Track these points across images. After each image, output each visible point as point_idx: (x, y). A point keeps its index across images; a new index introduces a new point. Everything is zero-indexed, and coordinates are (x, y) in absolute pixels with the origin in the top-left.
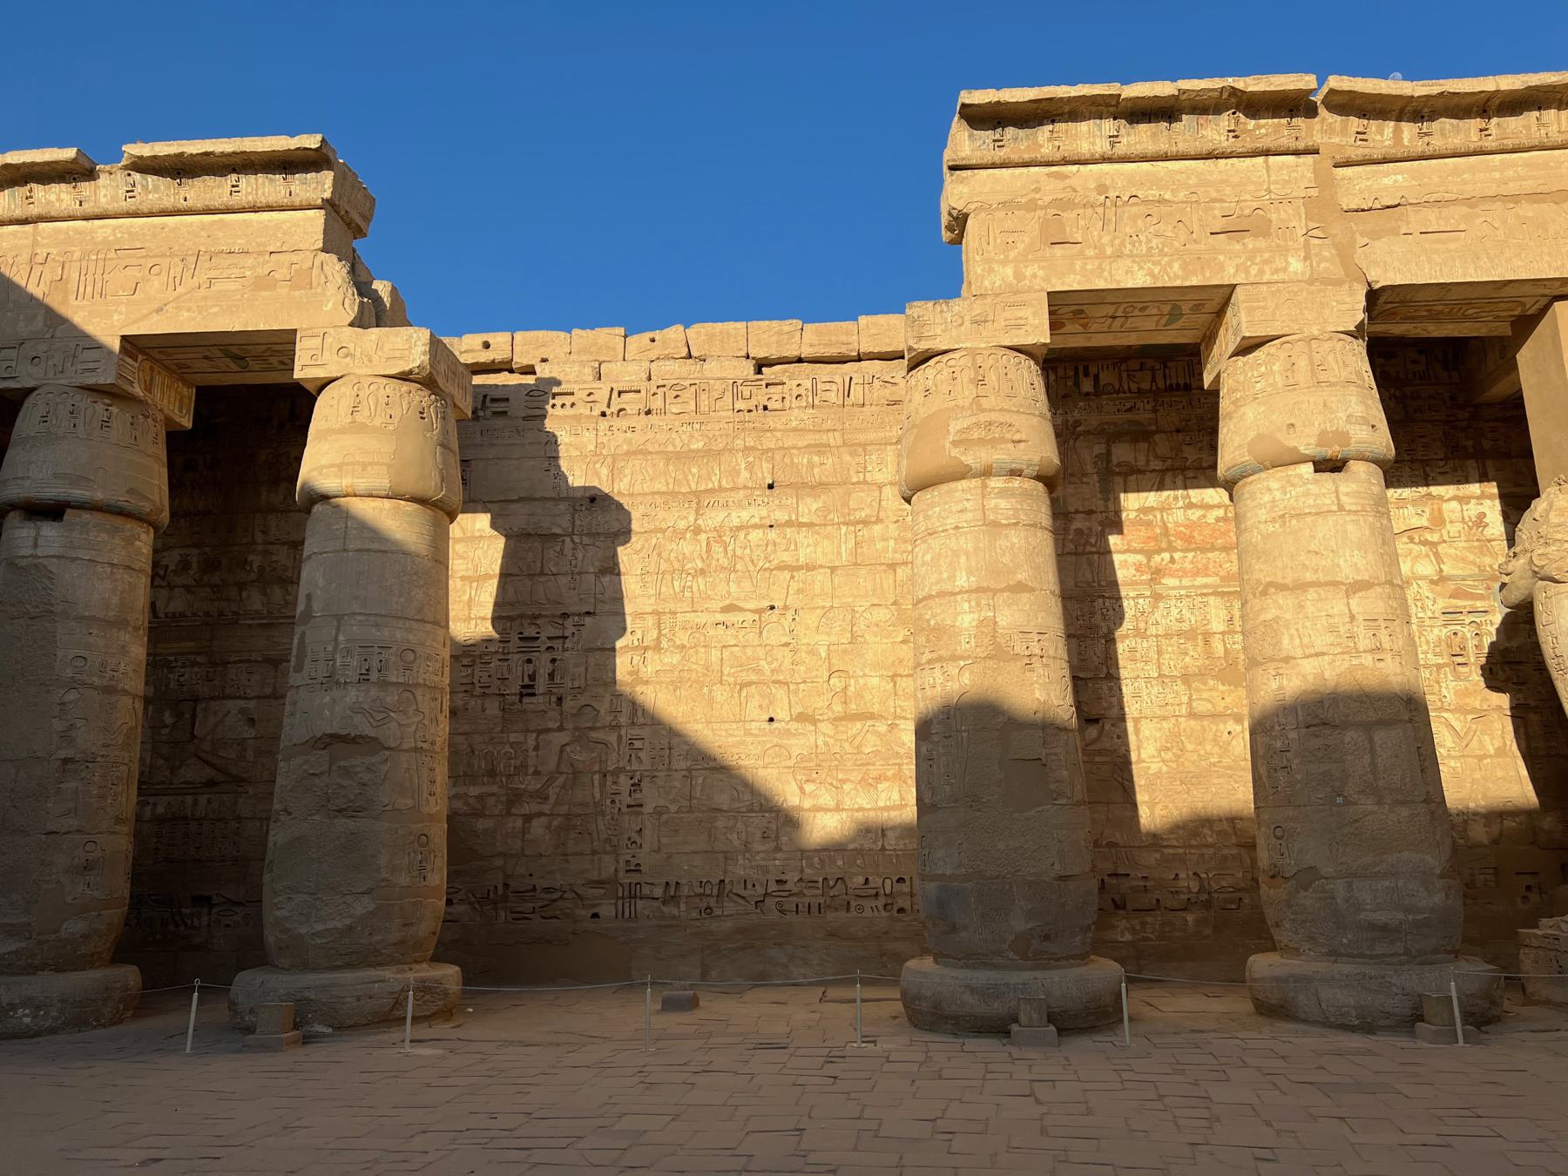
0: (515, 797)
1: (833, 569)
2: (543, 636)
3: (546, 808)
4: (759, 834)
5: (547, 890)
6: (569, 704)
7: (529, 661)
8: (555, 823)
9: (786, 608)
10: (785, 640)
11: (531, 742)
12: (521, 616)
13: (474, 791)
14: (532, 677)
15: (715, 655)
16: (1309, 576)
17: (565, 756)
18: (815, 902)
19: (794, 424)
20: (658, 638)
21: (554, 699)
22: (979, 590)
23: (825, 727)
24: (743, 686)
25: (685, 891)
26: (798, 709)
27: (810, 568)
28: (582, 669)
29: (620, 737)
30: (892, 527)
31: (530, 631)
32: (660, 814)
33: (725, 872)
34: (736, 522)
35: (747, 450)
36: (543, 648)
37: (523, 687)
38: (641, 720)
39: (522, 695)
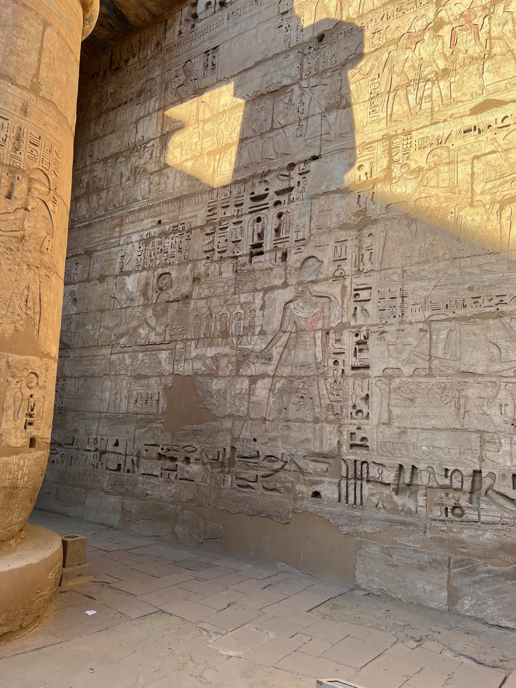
0: (243, 358)
2: (271, 193)
3: (270, 369)
5: (270, 458)
6: (293, 259)
7: (259, 220)
8: (278, 385)
11: (258, 302)
12: (253, 177)
13: (211, 352)
14: (260, 236)
15: (463, 170)
17: (288, 311)
20: (389, 169)
21: (279, 255)
25: (423, 479)
28: (307, 218)
29: (344, 287)
31: (260, 190)
32: (391, 378)
33: (482, 460)
36: (271, 205)
37: (254, 246)
38: (368, 266)
39: (252, 255)
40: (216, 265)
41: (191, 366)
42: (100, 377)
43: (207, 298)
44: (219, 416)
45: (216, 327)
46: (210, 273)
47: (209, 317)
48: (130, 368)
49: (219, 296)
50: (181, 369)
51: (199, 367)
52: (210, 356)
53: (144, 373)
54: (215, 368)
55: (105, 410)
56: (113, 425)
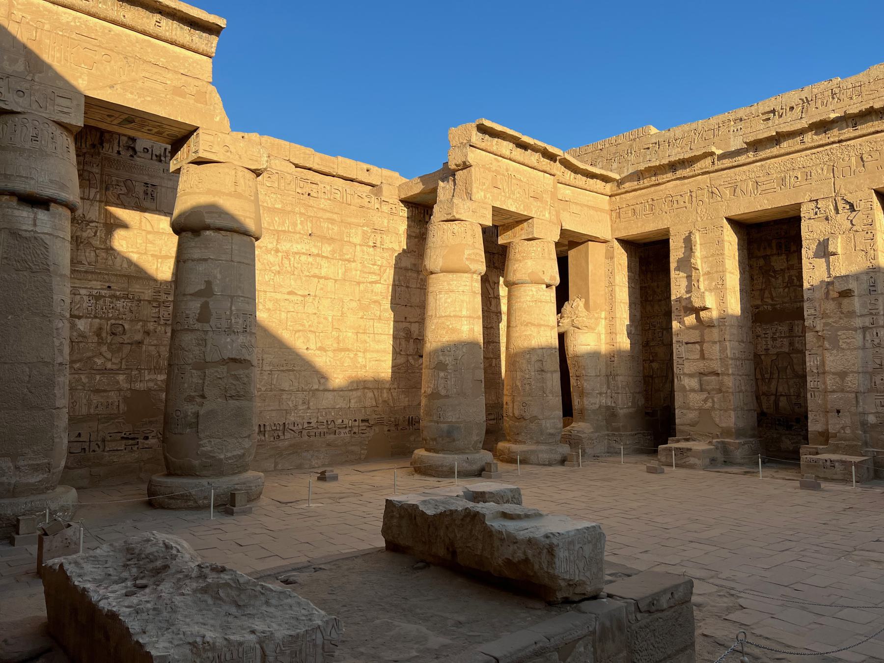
1: (336, 281)
4: (301, 402)
9: (315, 296)
10: (314, 311)
15: (283, 315)
16: (542, 322)
18: (322, 431)
19: (322, 206)
22: (470, 317)
23: (330, 354)
24: (296, 332)
25: (268, 428)
26: (319, 345)
27: (326, 278)
30: (359, 265)
34: (295, 250)
35: (301, 214)
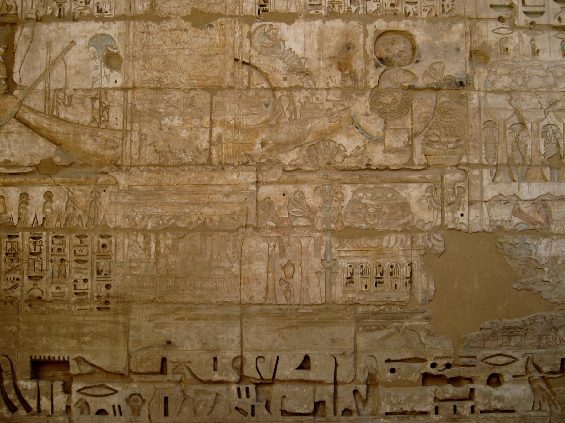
13: (530, 191)
40: (524, 36)
41: (486, 215)
42: (230, 232)
43: (509, 92)
44: (559, 301)
45: (535, 147)
46: (511, 47)
47: (518, 127)
48: (320, 214)
49: (537, 92)
50: (464, 220)
51: (506, 217)
52: (528, 197)
53: (364, 226)
54: (541, 220)
55: (259, 298)
56: (291, 327)
